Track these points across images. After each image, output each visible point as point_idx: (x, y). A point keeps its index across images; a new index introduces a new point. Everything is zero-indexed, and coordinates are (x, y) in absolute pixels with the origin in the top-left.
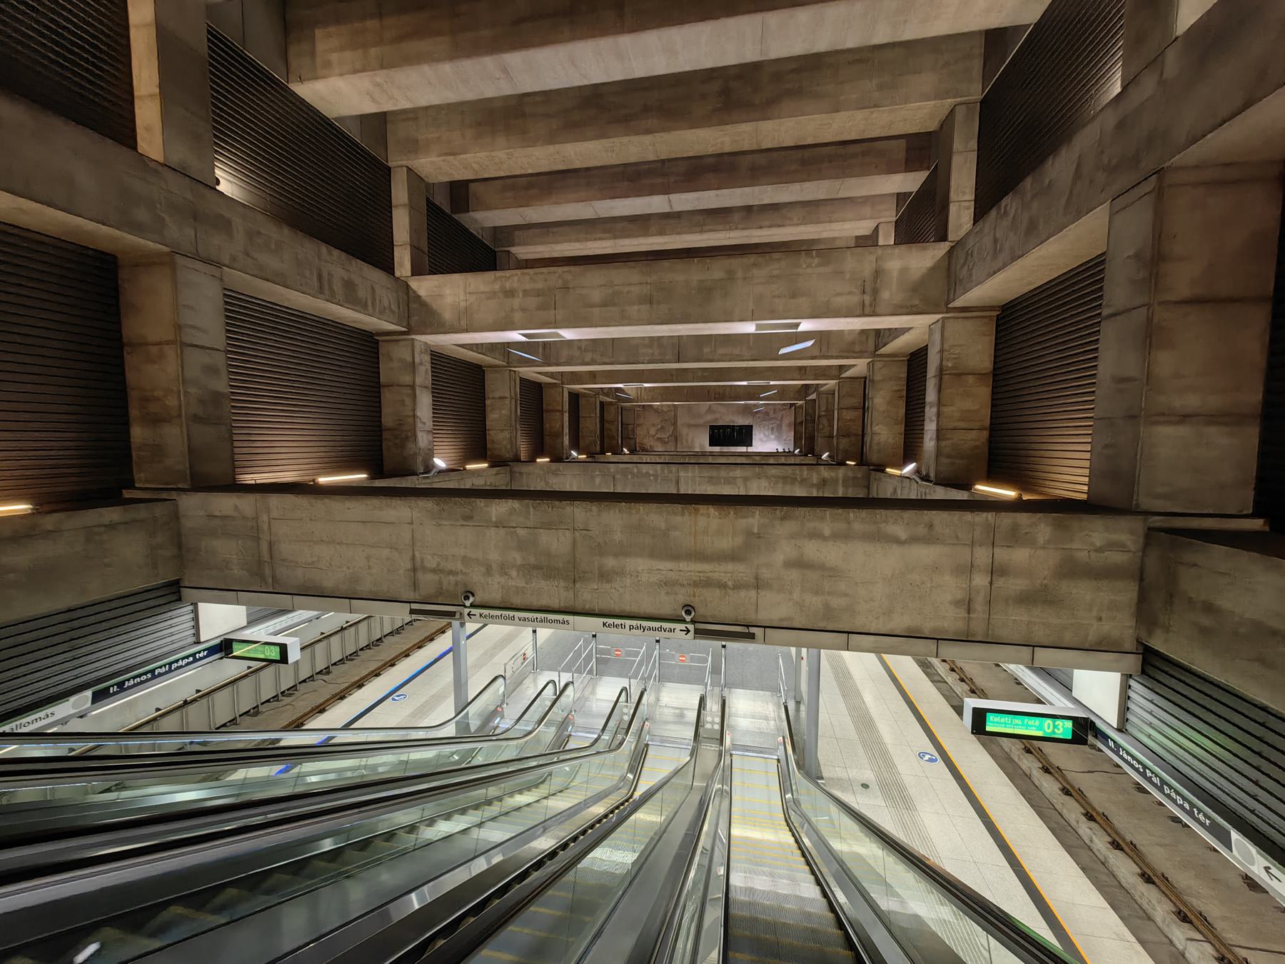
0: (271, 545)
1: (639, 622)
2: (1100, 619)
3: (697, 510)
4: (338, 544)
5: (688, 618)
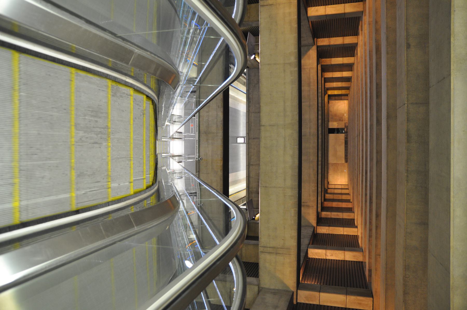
1: (198, 148)
3: (221, 161)
5: (199, 159)
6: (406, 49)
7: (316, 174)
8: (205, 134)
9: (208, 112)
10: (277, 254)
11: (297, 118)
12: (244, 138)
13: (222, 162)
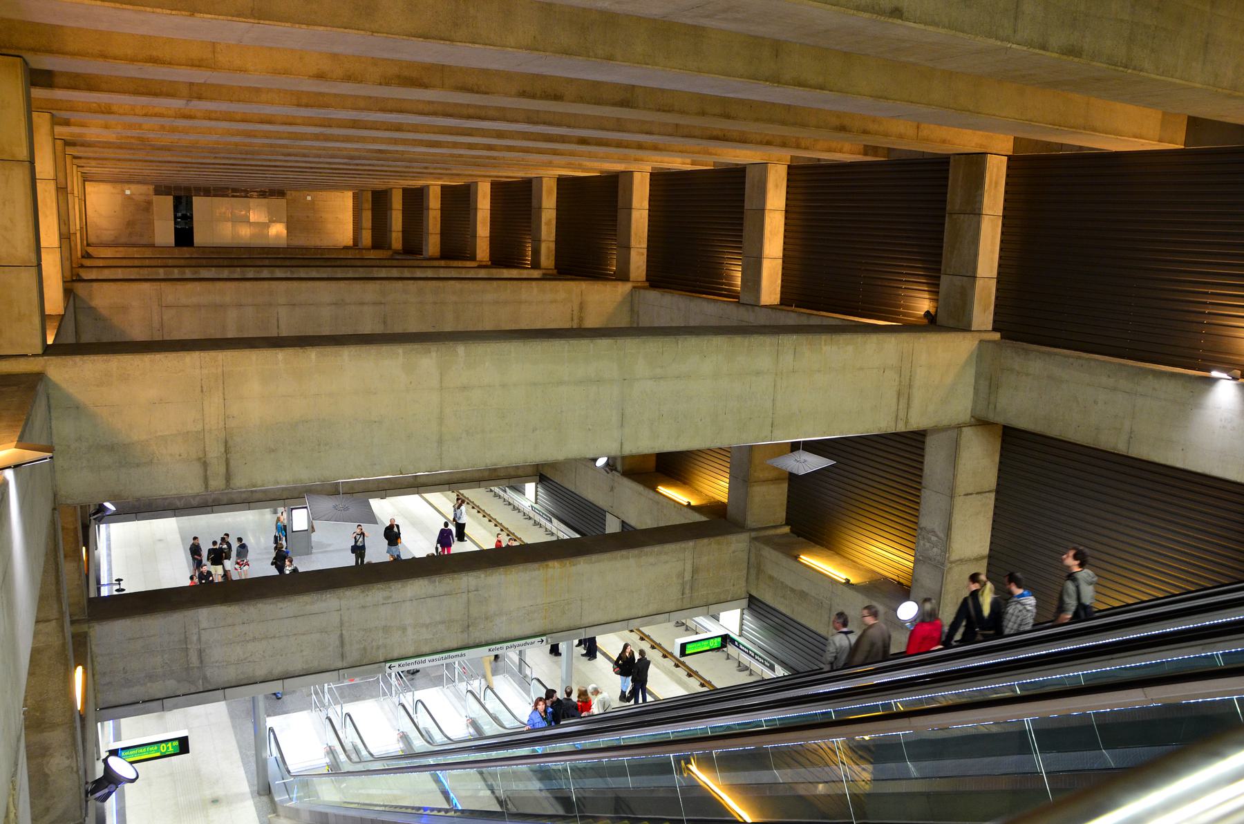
0: (200, 652)
1: (512, 643)
2: (734, 585)
3: (547, 565)
4: (271, 638)
6: (902, 20)
7: (495, 283)
8: (470, 629)
9: (404, 629)
10: (910, 386)
11: (604, 343)
12: (292, 509)
13: (551, 563)
